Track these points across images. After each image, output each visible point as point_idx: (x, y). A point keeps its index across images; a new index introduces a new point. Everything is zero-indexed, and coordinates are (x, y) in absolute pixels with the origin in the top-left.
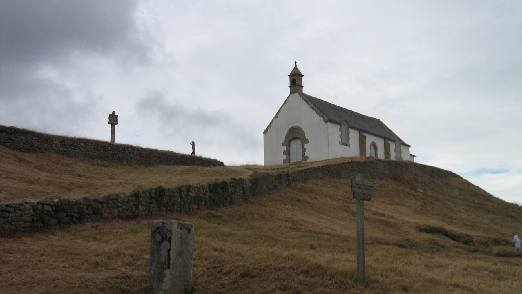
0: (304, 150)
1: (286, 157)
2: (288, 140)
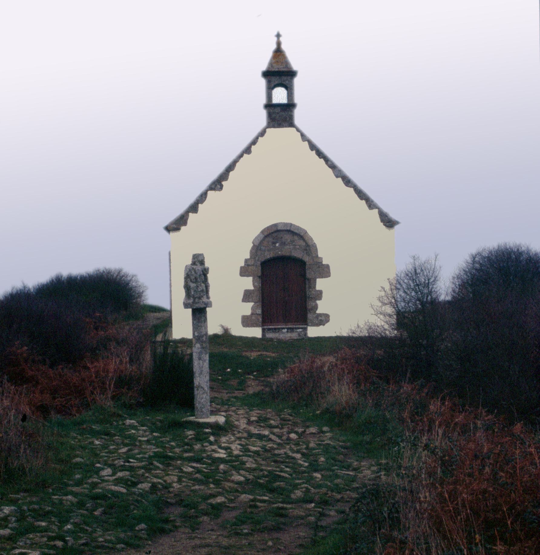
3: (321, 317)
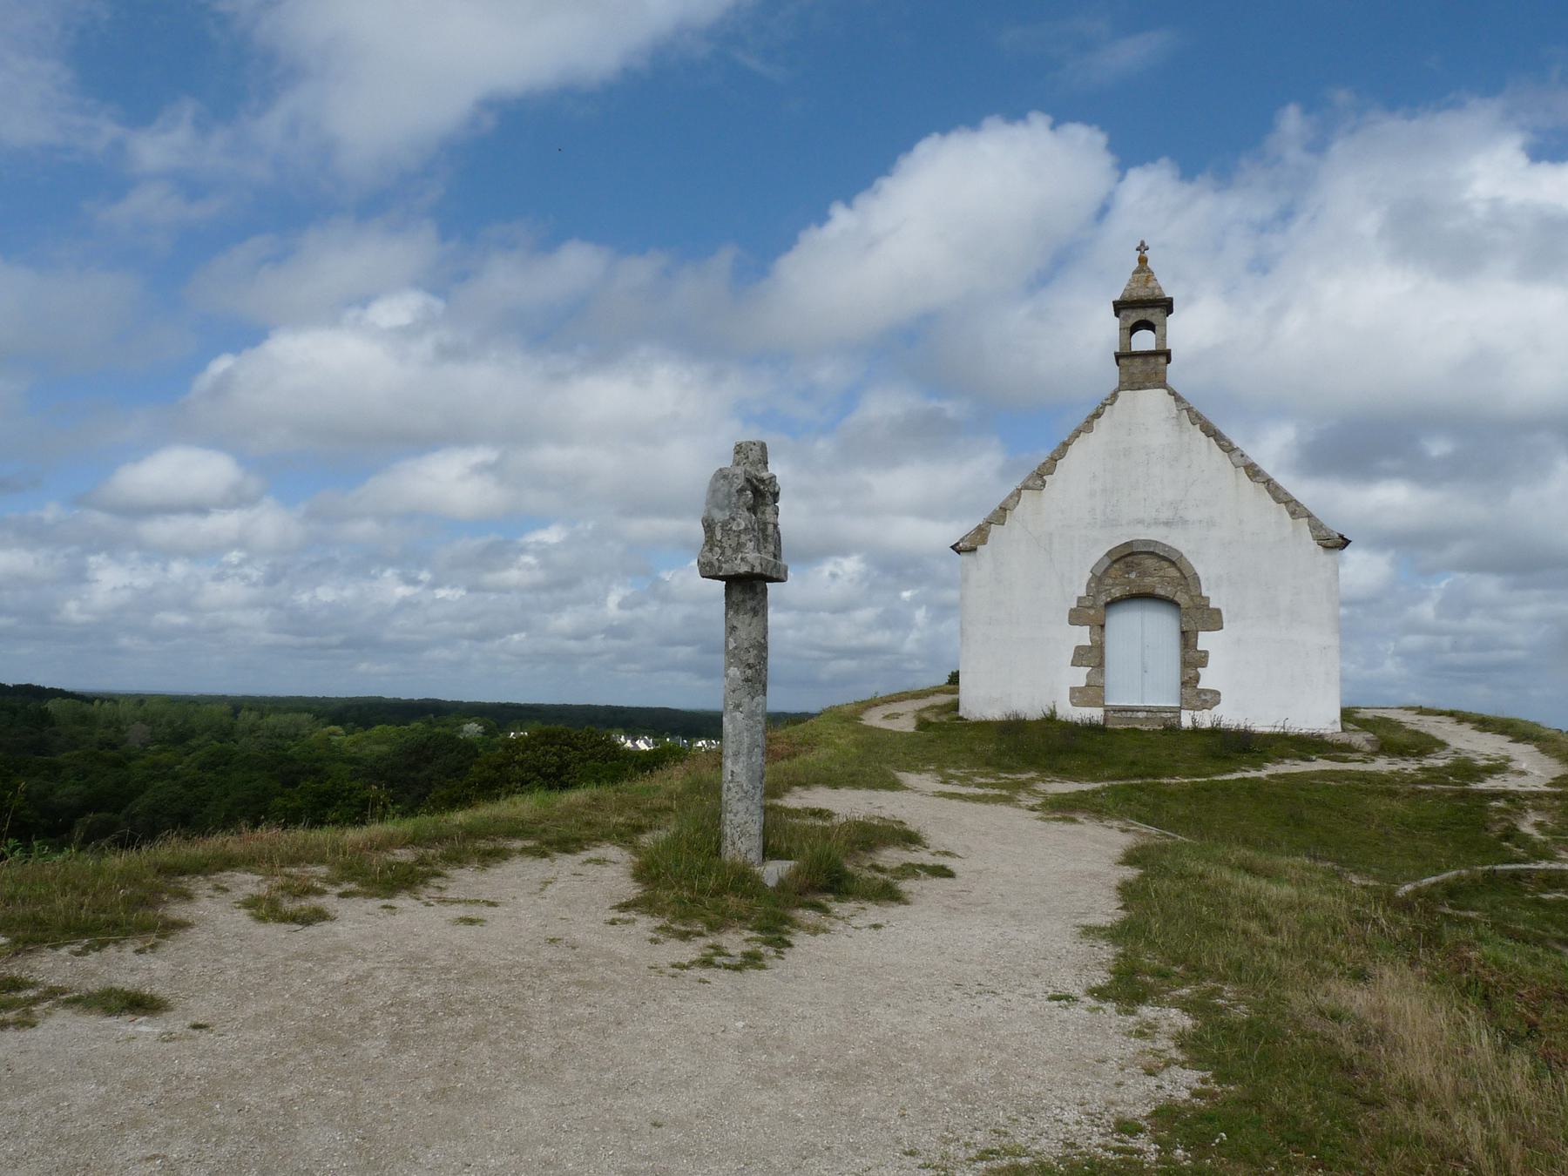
0: (1192, 660)
1: (1088, 675)
2: (1104, 598)
3: (1205, 695)
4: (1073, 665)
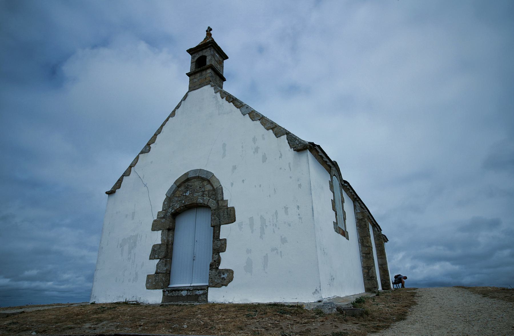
3: (224, 274)
4: (150, 259)
